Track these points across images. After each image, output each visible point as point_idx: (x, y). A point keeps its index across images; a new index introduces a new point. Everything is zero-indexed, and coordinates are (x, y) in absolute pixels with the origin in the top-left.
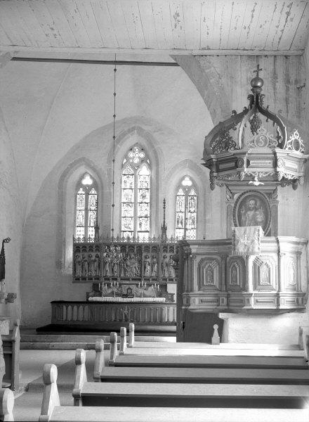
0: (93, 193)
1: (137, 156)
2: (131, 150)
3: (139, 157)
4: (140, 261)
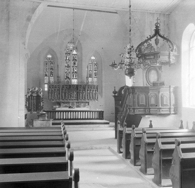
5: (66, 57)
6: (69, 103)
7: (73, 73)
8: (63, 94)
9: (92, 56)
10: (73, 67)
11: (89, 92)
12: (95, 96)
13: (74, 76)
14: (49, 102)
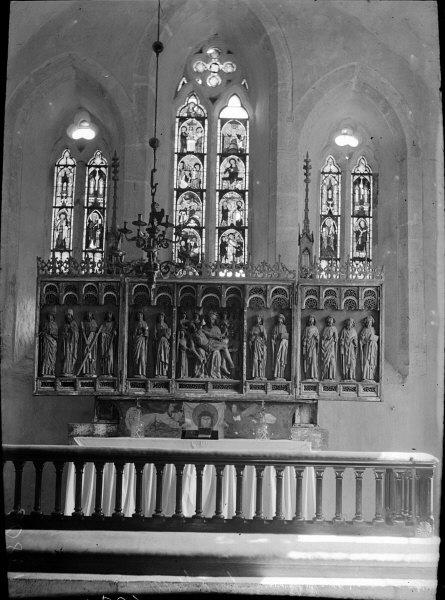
0: (98, 161)
1: (213, 69)
2: (201, 52)
3: (220, 72)
4: (236, 337)
5: (184, 137)
6: (178, 409)
7: (222, 230)
8: (142, 344)
9: (337, 130)
10: (222, 193)
11: (314, 330)
12: (360, 364)
13: (230, 250)
14: (46, 394)
